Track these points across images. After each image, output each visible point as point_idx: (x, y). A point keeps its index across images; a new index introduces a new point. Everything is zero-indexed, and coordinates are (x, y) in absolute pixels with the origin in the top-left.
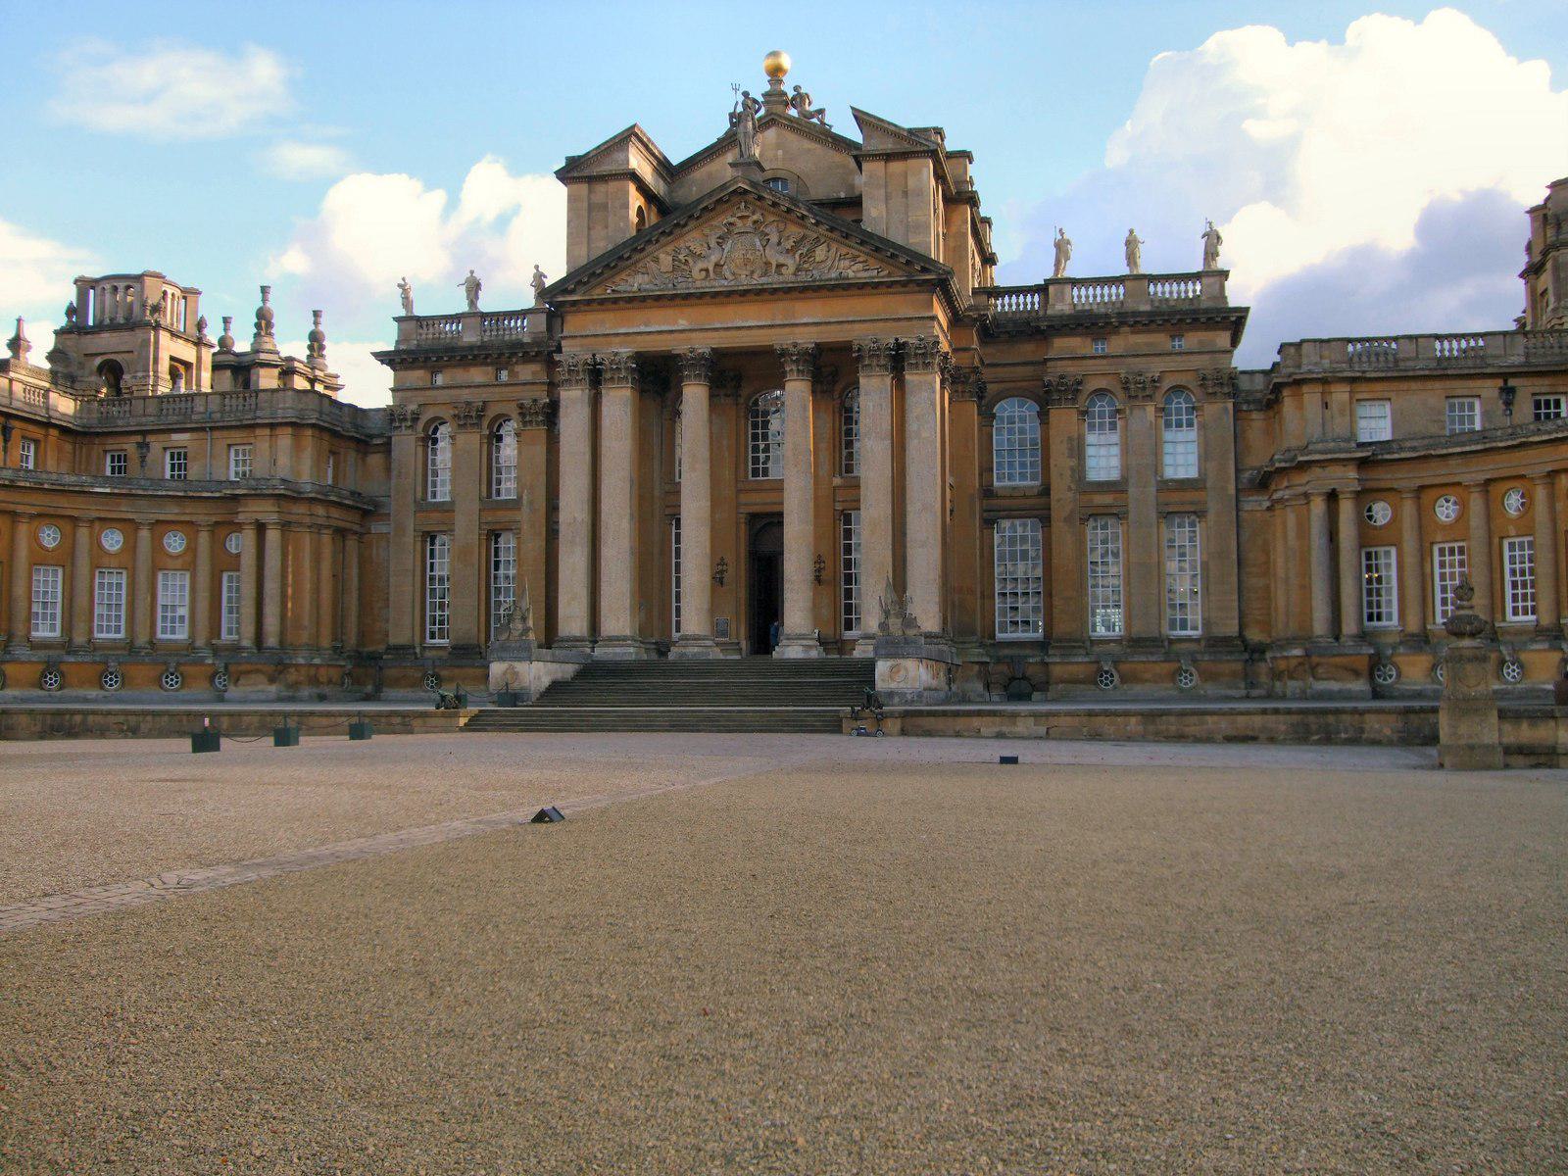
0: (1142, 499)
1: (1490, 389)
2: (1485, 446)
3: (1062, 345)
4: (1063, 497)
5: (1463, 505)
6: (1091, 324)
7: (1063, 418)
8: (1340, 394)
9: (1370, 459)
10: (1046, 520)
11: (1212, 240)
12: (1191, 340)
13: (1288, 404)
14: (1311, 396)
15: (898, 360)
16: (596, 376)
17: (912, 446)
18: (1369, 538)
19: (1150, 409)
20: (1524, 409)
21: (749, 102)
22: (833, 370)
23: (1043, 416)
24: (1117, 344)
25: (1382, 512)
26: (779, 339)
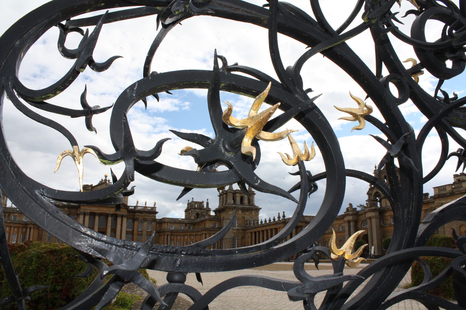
0: (144, 233)
1: (184, 225)
2: (184, 231)
3: (137, 214)
4: (135, 232)
5: (181, 238)
6: (140, 212)
7: (136, 223)
8: (169, 224)
9: (172, 232)
10: (133, 234)
11: (155, 204)
12: (152, 215)
13: (163, 224)
14: (166, 224)
15: (122, 217)
16: (85, 214)
17: (123, 226)
18: (171, 239)
19: (146, 223)
20: (187, 227)
21: (102, 180)
22: (115, 217)
23: (133, 222)
24: (143, 215)
25: (172, 238)
26: (109, 212)
